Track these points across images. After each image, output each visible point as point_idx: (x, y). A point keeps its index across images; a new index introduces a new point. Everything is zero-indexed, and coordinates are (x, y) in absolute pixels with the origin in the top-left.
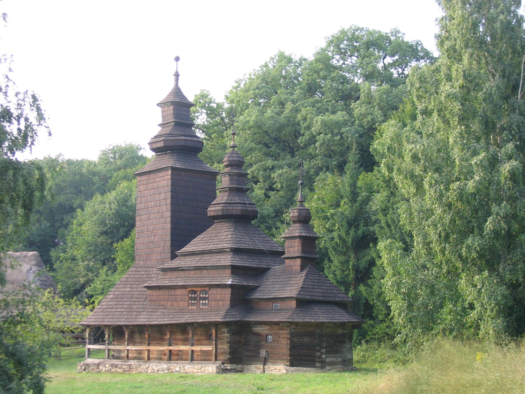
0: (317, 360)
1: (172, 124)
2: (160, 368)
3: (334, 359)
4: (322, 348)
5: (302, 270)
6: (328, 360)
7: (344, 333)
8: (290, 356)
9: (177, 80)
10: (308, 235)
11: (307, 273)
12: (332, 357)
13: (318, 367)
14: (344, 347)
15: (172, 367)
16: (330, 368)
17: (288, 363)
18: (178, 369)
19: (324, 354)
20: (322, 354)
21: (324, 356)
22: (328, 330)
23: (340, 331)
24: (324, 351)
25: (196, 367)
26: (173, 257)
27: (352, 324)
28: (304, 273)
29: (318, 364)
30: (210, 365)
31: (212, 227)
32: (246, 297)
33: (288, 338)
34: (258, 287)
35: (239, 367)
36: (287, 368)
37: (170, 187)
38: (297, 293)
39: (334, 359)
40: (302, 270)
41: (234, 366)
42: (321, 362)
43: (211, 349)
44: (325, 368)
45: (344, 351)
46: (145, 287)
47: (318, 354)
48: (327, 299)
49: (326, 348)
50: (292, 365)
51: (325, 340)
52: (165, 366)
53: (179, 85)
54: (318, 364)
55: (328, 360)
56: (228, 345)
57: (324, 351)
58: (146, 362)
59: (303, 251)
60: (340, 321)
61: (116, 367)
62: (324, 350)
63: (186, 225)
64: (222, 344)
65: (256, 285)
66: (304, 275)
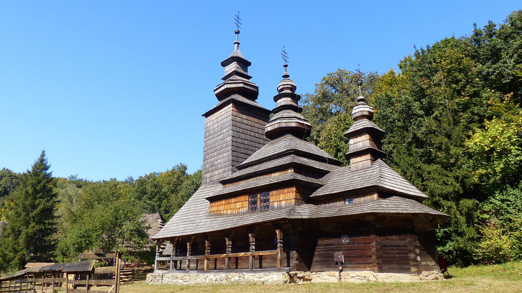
2: (217, 277)
4: (416, 247)
12: (426, 261)
15: (230, 277)
17: (376, 268)
18: (237, 278)
21: (419, 258)
25: (257, 275)
29: (413, 269)
30: (274, 273)
36: (375, 274)
42: (416, 266)
43: (276, 253)
46: (207, 199)
47: (412, 255)
50: (381, 270)
52: (223, 275)
55: (423, 263)
58: (206, 272)
61: (177, 277)
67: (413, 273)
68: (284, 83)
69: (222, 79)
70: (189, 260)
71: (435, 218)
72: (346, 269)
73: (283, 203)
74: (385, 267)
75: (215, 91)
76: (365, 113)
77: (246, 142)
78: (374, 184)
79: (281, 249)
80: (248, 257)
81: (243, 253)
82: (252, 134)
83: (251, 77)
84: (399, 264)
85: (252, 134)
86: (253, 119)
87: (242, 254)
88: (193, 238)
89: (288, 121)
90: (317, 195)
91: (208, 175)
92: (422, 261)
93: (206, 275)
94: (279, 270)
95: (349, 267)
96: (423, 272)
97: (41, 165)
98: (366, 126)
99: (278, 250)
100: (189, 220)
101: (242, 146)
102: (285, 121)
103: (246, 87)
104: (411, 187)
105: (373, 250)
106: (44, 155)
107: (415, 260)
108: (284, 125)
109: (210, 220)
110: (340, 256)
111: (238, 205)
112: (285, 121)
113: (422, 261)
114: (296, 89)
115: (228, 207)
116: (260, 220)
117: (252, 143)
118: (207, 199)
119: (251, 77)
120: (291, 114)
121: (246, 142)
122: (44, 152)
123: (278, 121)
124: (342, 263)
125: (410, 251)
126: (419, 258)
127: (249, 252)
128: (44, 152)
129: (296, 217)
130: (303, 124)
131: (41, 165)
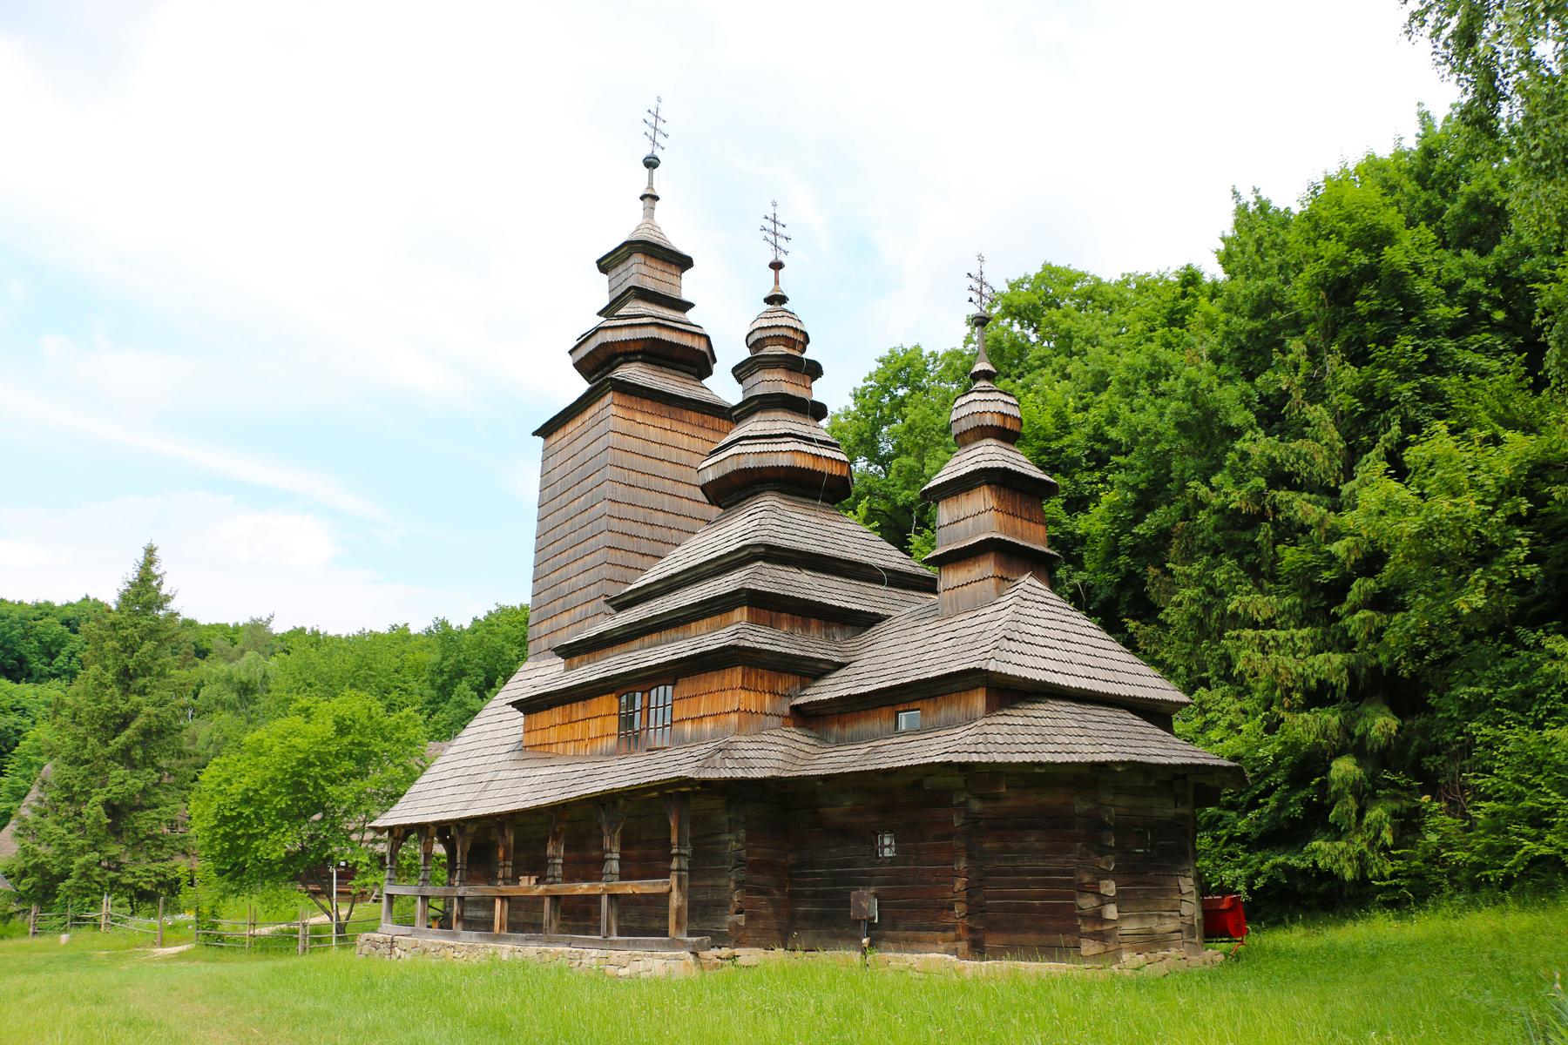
0: (1085, 928)
4: (1106, 875)
12: (1142, 918)
17: (963, 946)
19: (1112, 900)
20: (1104, 900)
21: (1111, 912)
23: (1167, 810)
29: (1089, 947)
34: (841, 666)
42: (1101, 937)
43: (665, 889)
44: (1117, 960)
46: (514, 704)
47: (1088, 903)
51: (1112, 843)
55: (1130, 927)
61: (425, 951)
62: (1113, 885)
65: (837, 659)
67: (1085, 959)
68: (765, 323)
69: (600, 314)
70: (461, 899)
71: (1176, 777)
72: (883, 944)
73: (708, 725)
74: (992, 941)
75: (571, 352)
76: (988, 420)
77: (660, 518)
78: (972, 666)
79: (680, 879)
80: (599, 896)
81: (585, 885)
83: (691, 305)
84: (1041, 931)
86: (685, 441)
87: (583, 888)
88: (471, 829)
89: (765, 448)
90: (814, 698)
91: (545, 627)
92: (1121, 918)
93: (492, 946)
94: (675, 945)
95: (895, 940)
96: (1126, 957)
97: (144, 591)
98: (982, 465)
99: (673, 881)
100: (471, 771)
101: (645, 531)
102: (758, 448)
103: (666, 335)
104: (1129, 667)
105: (959, 884)
106: (152, 563)
107: (1098, 917)
108: (752, 463)
109: (515, 774)
110: (868, 904)
111: (594, 727)
112: (758, 448)
113: (1121, 918)
114: (807, 340)
116: (552, 796)
118: (514, 704)
119: (691, 305)
120: (779, 425)
121: (660, 518)
122: (150, 551)
123: (735, 450)
124: (871, 926)
125: (1083, 890)
126: (1111, 912)
127: (600, 880)
128: (150, 551)
129: (727, 774)
131: (144, 591)
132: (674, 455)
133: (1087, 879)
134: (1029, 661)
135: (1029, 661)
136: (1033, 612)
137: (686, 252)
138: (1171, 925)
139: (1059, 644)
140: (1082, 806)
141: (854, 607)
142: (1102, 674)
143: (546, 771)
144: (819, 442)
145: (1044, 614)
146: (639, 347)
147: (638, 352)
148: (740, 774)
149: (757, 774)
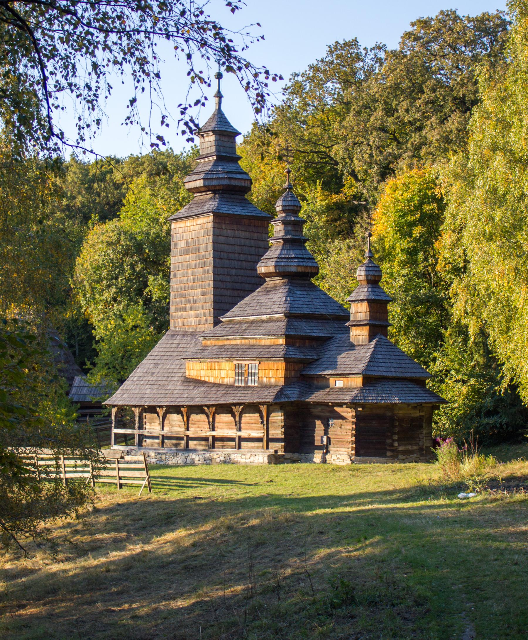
1: (214, 158)
3: (409, 447)
4: (395, 434)
5: (370, 341)
6: (401, 448)
7: (421, 416)
8: (356, 442)
9: (220, 103)
10: (377, 298)
11: (376, 344)
12: (405, 445)
13: (389, 457)
14: (422, 433)
16: (404, 457)
17: (353, 452)
19: (396, 440)
20: (394, 441)
21: (396, 444)
22: (401, 412)
23: (416, 414)
24: (396, 437)
26: (217, 322)
27: (430, 405)
28: (373, 342)
29: (389, 454)
31: (263, 286)
32: (304, 373)
33: (353, 422)
34: (317, 360)
35: (296, 456)
37: (211, 237)
38: (363, 368)
39: (409, 447)
40: (370, 341)
41: (289, 455)
42: (393, 451)
45: (421, 437)
47: (389, 441)
48: (399, 375)
49: (398, 434)
51: (397, 424)
53: (223, 108)
54: (389, 454)
55: (401, 448)
56: (283, 430)
57: (396, 437)
59: (372, 317)
60: (417, 401)
62: (397, 436)
63: (232, 284)
64: (275, 429)
65: (316, 358)
66: (372, 346)
82: (242, 257)
85: (242, 257)
86: (242, 234)
96: (400, 456)
101: (228, 278)
103: (233, 183)
107: (392, 445)
115: (209, 373)
117: (242, 272)
121: (233, 272)
126: (396, 444)
129: (283, 400)
130: (306, 266)
132: (238, 241)
133: (389, 434)
134: (376, 369)
135: (376, 369)
136: (380, 349)
137: (239, 130)
138: (415, 448)
139: (387, 361)
140: (389, 414)
141: (321, 335)
142: (401, 370)
143: (203, 388)
144: (307, 258)
145: (384, 350)
146: (221, 188)
147: (219, 190)
148: (287, 400)
149: (292, 400)
